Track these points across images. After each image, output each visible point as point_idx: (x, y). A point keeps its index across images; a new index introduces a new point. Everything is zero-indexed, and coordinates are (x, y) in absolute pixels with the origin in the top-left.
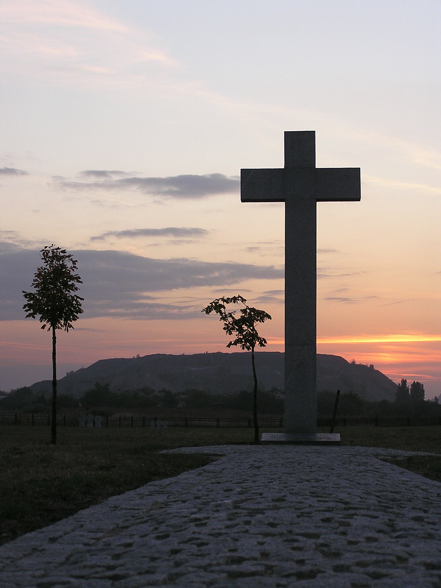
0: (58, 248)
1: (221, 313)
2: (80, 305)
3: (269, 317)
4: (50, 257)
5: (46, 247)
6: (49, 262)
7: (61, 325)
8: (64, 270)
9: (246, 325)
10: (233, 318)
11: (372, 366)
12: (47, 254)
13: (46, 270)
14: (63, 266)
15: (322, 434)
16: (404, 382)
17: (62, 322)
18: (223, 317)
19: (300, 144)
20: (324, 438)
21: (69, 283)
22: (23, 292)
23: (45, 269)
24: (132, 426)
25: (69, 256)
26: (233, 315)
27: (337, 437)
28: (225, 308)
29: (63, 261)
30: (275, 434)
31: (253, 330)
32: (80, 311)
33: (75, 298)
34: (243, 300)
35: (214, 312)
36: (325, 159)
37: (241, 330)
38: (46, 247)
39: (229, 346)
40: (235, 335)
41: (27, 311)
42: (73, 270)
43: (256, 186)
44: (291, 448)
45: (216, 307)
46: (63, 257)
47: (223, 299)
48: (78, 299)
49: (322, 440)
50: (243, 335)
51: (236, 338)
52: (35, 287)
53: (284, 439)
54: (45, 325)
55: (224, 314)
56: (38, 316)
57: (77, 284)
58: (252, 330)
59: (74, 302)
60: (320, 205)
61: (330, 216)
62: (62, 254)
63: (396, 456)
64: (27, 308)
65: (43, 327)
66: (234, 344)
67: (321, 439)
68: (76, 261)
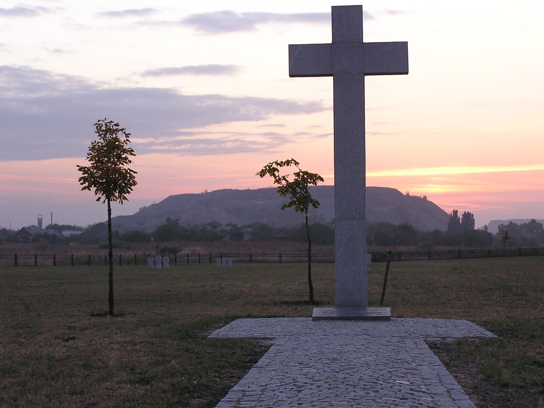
0: (111, 122)
1: (275, 177)
2: (134, 177)
3: (322, 180)
4: (103, 131)
5: (99, 121)
6: (103, 136)
7: (116, 197)
8: (117, 143)
9: (300, 188)
10: (287, 181)
11: (425, 197)
12: (101, 128)
13: (100, 144)
14: (117, 139)
15: (372, 308)
16: (455, 212)
17: (117, 194)
18: (277, 180)
19: (347, 20)
20: (375, 313)
21: (123, 156)
22: (78, 166)
23: (98, 143)
24: (200, 262)
25: (122, 130)
26: (287, 178)
27: (387, 311)
28: (278, 171)
29: (116, 134)
30: (326, 309)
31: (307, 192)
32: (135, 183)
33: (129, 171)
34: (296, 163)
35: (268, 175)
36: (372, 33)
37: (294, 193)
38: (99, 121)
39: (283, 208)
40: (288, 198)
41: (82, 184)
42: (127, 144)
43: (304, 61)
44: (341, 323)
45: (270, 170)
46: (116, 130)
47: (276, 163)
48: (131, 173)
49: (372, 315)
50: (297, 198)
51: (290, 200)
52: (89, 161)
53: (334, 315)
54: (100, 198)
55: (277, 178)
56: (93, 189)
57: (130, 157)
58: (305, 193)
59: (128, 175)
60: (368, 79)
61: (377, 88)
62: (115, 128)
63: (445, 338)
64: (82, 181)
65: (98, 200)
66: (288, 206)
67: (371, 314)
68: (130, 134)
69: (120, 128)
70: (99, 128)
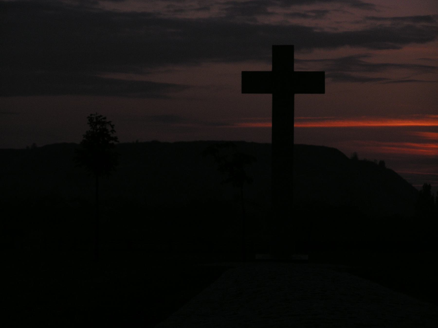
0: (101, 116)
8: (105, 132)
19: (283, 55)
25: (110, 122)
38: (91, 115)
42: (113, 133)
43: (252, 83)
62: (103, 120)
68: (114, 125)
69: (107, 120)
70: (90, 119)
